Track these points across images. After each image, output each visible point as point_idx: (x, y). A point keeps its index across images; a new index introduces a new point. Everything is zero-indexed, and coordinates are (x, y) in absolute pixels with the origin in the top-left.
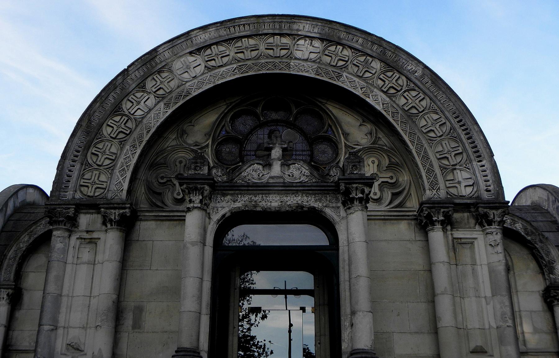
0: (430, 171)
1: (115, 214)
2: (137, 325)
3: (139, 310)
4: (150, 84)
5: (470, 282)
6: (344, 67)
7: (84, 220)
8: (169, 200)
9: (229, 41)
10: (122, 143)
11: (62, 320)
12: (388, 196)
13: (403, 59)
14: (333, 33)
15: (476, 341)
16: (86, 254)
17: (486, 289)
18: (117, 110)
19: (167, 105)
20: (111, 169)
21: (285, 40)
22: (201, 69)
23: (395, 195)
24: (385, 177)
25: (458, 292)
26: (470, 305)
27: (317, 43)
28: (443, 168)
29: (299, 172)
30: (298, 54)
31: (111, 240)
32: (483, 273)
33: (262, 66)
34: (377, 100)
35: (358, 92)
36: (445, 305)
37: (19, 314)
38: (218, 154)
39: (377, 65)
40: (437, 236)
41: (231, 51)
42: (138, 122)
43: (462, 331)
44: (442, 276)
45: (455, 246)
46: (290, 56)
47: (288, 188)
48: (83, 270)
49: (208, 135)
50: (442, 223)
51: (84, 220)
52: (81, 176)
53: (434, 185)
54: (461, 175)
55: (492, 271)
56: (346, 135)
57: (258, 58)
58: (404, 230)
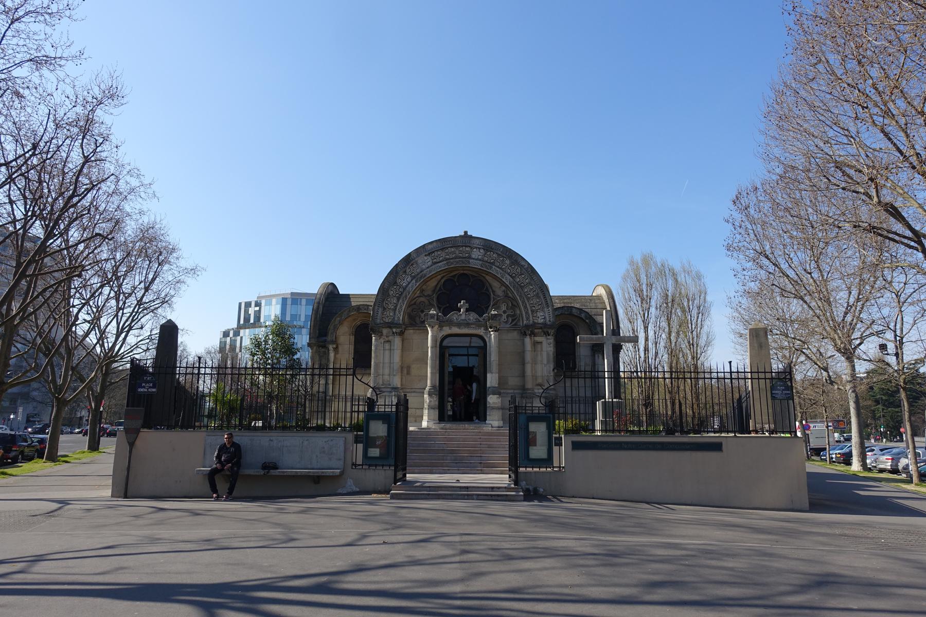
0: (527, 313)
1: (398, 330)
2: (408, 373)
3: (409, 368)
4: (408, 271)
5: (539, 358)
6: (493, 264)
7: (385, 331)
8: (418, 321)
9: (442, 249)
10: (398, 299)
11: (381, 372)
12: (510, 320)
13: (520, 260)
14: (489, 246)
15: (540, 381)
16: (387, 346)
17: (545, 362)
18: (395, 283)
19: (416, 282)
20: (395, 310)
21: (467, 249)
22: (430, 264)
23: (513, 321)
24: (509, 312)
25: (534, 362)
26: (539, 367)
27: (482, 251)
28: (533, 311)
29: (473, 316)
30: (473, 256)
31: (397, 341)
32: (545, 354)
33: (457, 263)
34: (507, 280)
35: (499, 276)
36: (528, 368)
37: (338, 356)
38: (438, 299)
39: (508, 262)
40: (528, 340)
41: (443, 255)
42: (404, 289)
43: (535, 377)
44: (528, 357)
45: (535, 344)
46: (470, 257)
47: (467, 325)
48: (387, 352)
49: (434, 291)
50: (530, 335)
51: (385, 331)
52: (383, 314)
53: (528, 319)
54: (540, 314)
55: (548, 354)
56: (494, 292)
57: (456, 258)
58: (515, 335)
